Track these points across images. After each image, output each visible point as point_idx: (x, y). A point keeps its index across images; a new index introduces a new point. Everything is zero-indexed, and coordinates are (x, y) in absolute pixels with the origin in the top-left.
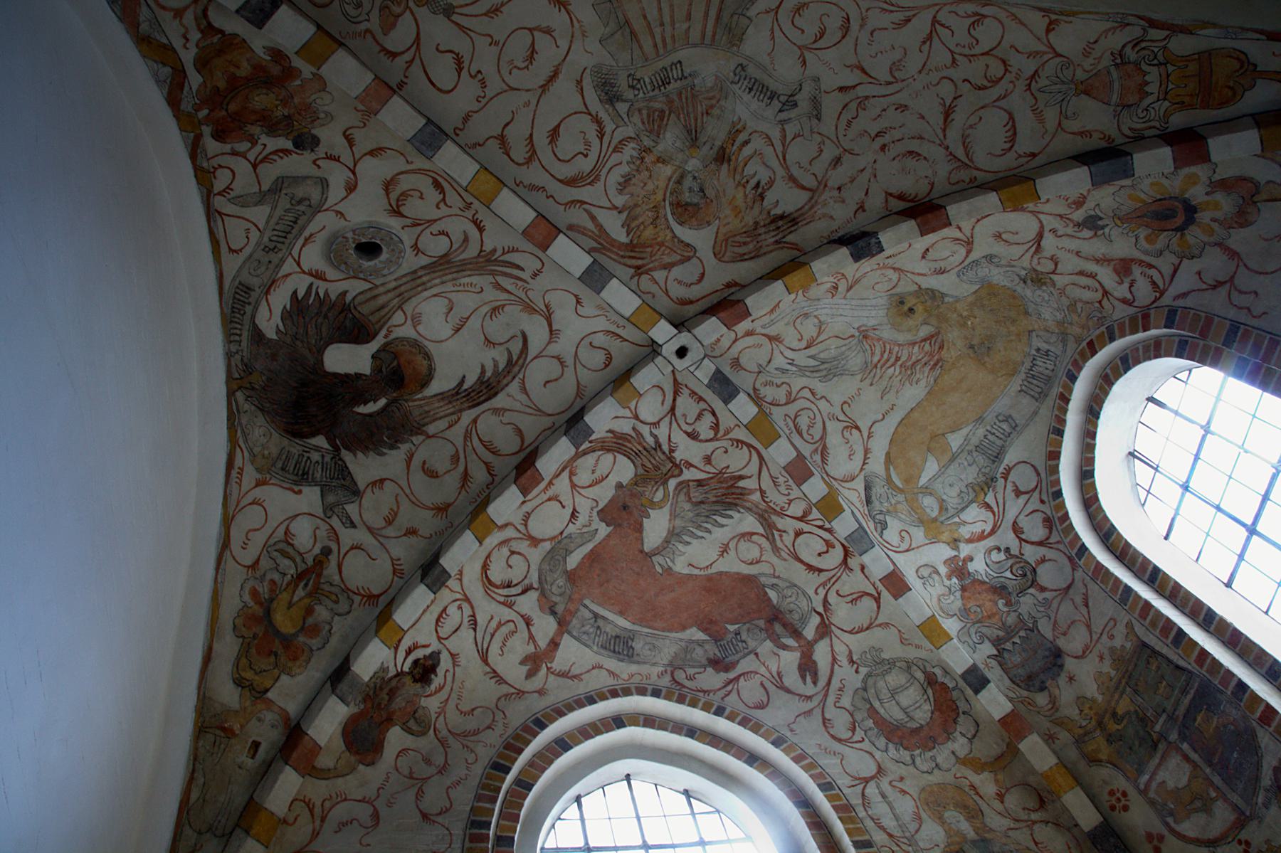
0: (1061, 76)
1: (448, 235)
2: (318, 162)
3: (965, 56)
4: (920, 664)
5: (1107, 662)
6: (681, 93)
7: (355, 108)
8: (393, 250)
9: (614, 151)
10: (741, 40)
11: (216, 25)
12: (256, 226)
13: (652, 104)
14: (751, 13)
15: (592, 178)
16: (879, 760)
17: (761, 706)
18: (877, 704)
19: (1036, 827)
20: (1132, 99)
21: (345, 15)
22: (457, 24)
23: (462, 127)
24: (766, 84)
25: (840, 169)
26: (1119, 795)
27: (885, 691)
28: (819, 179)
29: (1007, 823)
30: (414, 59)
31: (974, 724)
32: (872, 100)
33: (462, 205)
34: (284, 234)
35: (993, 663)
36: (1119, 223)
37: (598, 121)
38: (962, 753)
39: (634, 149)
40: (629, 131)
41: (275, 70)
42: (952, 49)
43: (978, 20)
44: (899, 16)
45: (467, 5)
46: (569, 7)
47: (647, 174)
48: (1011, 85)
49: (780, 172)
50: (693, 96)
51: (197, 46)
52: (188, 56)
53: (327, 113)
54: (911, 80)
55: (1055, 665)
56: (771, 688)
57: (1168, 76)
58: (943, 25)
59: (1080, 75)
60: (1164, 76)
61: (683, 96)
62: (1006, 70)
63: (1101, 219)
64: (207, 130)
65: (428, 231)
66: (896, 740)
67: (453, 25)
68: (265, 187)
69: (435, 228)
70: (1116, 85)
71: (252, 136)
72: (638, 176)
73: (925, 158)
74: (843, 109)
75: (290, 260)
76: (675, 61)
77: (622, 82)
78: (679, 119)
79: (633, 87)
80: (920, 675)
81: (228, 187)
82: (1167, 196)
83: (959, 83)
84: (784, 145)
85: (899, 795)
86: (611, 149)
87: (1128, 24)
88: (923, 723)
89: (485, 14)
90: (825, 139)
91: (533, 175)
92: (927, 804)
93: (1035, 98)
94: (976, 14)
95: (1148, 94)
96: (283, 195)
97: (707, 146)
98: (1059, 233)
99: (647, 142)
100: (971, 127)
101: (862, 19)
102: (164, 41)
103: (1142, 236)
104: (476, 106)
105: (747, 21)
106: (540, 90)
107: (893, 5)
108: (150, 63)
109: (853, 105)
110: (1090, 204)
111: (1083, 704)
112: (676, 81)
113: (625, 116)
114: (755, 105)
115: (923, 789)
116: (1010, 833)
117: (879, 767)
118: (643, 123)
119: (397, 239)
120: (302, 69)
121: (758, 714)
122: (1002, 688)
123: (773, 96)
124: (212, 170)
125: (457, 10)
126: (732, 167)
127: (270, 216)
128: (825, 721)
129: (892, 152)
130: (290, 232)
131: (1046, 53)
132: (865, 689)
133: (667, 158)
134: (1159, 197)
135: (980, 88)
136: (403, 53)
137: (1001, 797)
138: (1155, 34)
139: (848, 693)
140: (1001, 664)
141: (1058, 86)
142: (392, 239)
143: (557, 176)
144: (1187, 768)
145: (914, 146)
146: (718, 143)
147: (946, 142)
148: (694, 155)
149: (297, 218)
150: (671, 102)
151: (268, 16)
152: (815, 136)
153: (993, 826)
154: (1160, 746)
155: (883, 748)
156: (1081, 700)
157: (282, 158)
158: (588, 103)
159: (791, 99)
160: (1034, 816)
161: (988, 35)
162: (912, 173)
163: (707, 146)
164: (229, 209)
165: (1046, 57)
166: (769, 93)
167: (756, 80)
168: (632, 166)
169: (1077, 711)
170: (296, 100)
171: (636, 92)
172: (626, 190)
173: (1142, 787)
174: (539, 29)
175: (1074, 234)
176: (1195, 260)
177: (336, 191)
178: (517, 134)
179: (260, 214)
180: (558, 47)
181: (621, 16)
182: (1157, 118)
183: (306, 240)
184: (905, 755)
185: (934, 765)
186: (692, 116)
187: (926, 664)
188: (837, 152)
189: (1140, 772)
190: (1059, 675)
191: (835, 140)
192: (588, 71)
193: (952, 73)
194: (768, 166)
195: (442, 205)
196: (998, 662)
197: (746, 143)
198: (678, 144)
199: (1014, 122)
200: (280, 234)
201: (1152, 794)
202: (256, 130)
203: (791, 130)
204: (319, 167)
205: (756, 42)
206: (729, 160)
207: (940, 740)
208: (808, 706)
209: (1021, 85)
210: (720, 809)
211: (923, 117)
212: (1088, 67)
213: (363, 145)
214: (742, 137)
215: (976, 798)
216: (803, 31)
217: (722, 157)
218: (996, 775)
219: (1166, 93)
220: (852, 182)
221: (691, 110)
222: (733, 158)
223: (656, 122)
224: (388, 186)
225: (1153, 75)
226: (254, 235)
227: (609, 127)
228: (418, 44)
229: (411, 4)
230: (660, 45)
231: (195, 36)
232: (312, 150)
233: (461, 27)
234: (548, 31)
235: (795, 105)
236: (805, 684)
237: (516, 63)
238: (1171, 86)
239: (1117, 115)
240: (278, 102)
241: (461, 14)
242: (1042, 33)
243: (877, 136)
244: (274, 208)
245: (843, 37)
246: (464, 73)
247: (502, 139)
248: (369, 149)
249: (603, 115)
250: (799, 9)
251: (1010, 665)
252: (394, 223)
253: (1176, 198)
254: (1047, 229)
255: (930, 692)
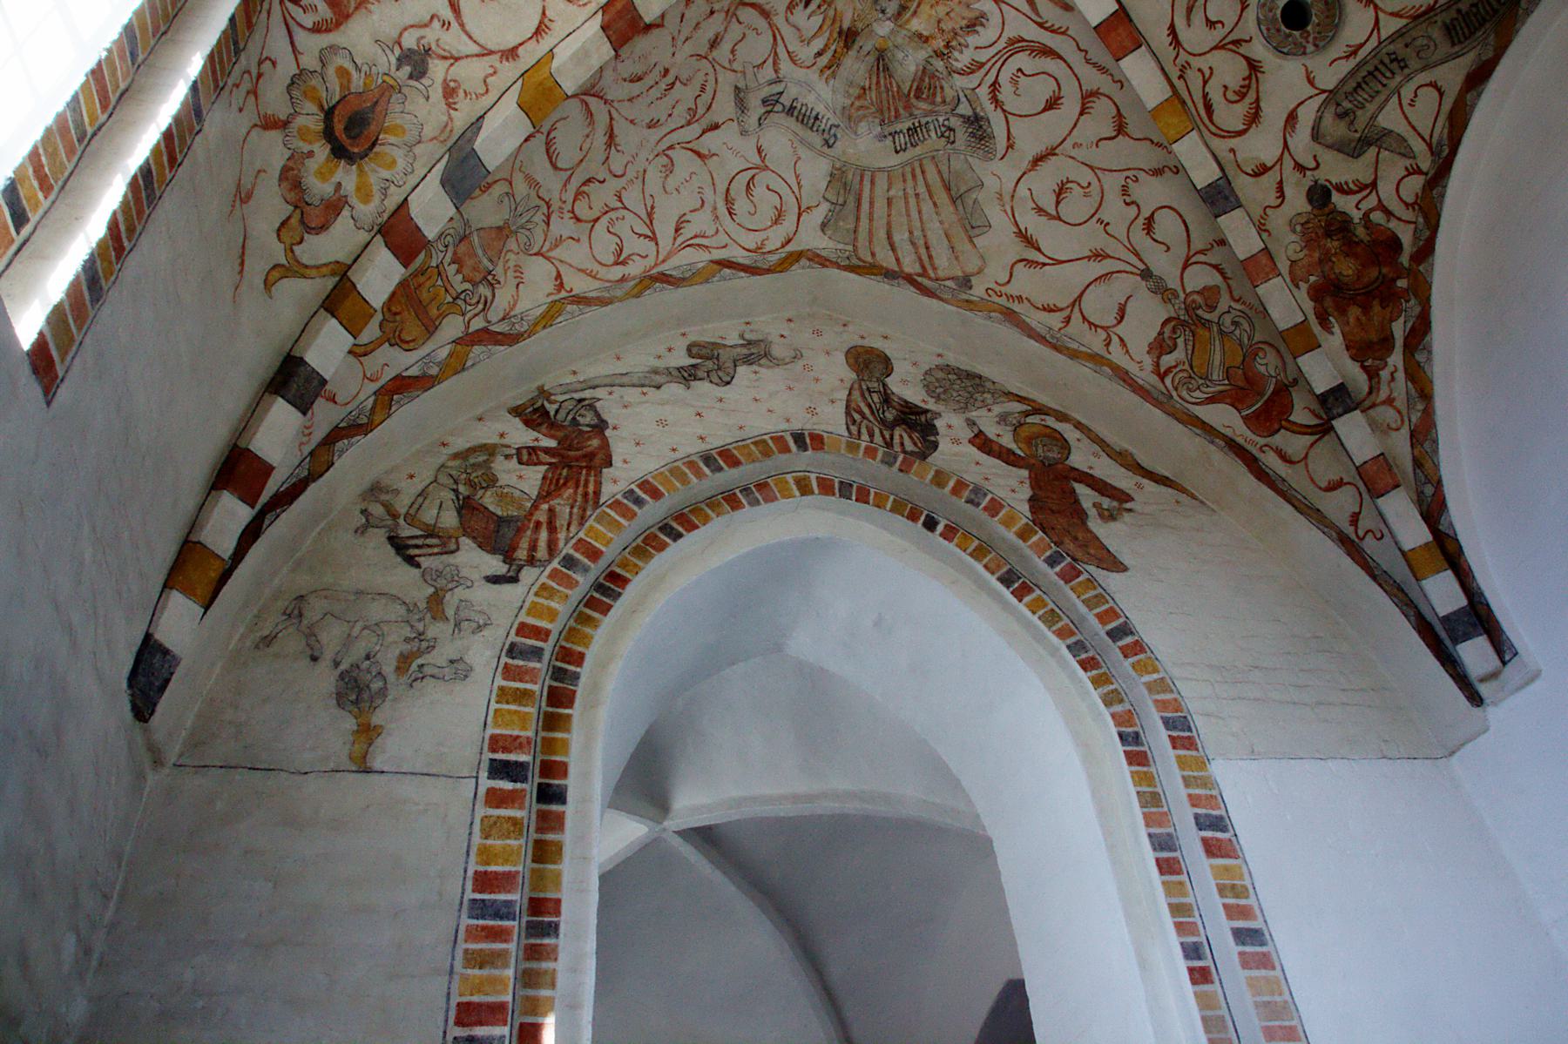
0: (528, 233)
1: (1207, 19)
2: (1313, 165)
3: (613, 210)
6: (896, 117)
7: (1270, 235)
8: (1270, 11)
9: (982, 65)
10: (831, 175)
11: (1365, 377)
12: (1400, 104)
13: (930, 107)
14: (825, 207)
15: (1017, 45)
20: (462, 248)
21: (1252, 325)
22: (1141, 260)
23: (1166, 169)
24: (799, 124)
25: (711, 35)
28: (734, 20)
30: (1196, 254)
32: (683, 122)
33: (1189, 73)
34: (1376, 73)
36: (392, 82)
37: (997, 102)
39: (957, 60)
40: (960, 82)
41: (1328, 302)
42: (626, 211)
43: (619, 256)
44: (688, 232)
45: (1127, 272)
46: (1016, 230)
47: (942, 25)
48: (564, 199)
49: (779, 21)
50: (881, 111)
51: (1386, 364)
52: (1396, 359)
53: (1294, 231)
54: (651, 158)
57: (446, 290)
58: (646, 237)
59: (512, 244)
60: (449, 287)
61: (893, 113)
62: (573, 212)
63: (411, 77)
64: (1405, 260)
65: (1227, 29)
67: (1146, 261)
68: (1373, 150)
69: (1219, 32)
70: (480, 252)
71: (1367, 228)
72: (957, 27)
73: (625, 80)
74: (711, 104)
75: (1384, 35)
76: (901, 153)
77: (962, 136)
78: (899, 87)
79: (951, 129)
81: (1410, 174)
82: (371, 155)
83: (609, 177)
84: (776, 53)
86: (987, 67)
87: (503, 319)
89: (1109, 256)
90: (727, 65)
91: (1092, 79)
93: (539, 197)
94: (624, 263)
95: (453, 262)
96: (1360, 130)
97: (864, 52)
98: (436, 24)
99: (939, 64)
100: (588, 136)
101: (717, 217)
102: (1409, 383)
103: (353, 72)
104: (1141, 175)
105: (828, 196)
106: (1057, 151)
107: (698, 245)
108: (1429, 374)
109: (700, 111)
110: (437, 93)
112: (901, 131)
113: (963, 99)
114: (810, 100)
118: (942, 88)
119: (1263, 28)
120: (1306, 295)
123: (790, 111)
124: (1416, 207)
125: (1139, 272)
126: (837, 25)
127: (1381, 108)
129: (659, 68)
130: (1370, 73)
131: (548, 251)
133: (916, 39)
134: (377, 149)
135: (589, 181)
136: (1205, 263)
138: (477, 324)
141: (524, 221)
142: (1268, 30)
143: (1064, 65)
145: (636, 88)
146: (852, 53)
147: (608, 106)
148: (881, 40)
149: (1355, 90)
150: (908, 107)
151: (1332, 391)
152: (740, 69)
157: (1346, 183)
158: (1004, 122)
159: (769, 108)
161: (604, 245)
162: (637, 59)
163: (864, 52)
164: (1418, 146)
165: (547, 245)
166: (796, 113)
167: (811, 128)
168: (963, 41)
170: (1316, 255)
171: (946, 123)
172: (972, 15)
174: (1051, 217)
175: (422, 32)
176: (289, 81)
177: (1307, 116)
178: (1099, 122)
179: (1390, 118)
180: (1030, 189)
181: (960, 208)
182: (434, 245)
183: (1355, 53)
186: (883, 88)
188: (715, 53)
191: (717, 67)
192: (999, 155)
193: (616, 184)
194: (794, 26)
195: (1207, 75)
197: (819, 54)
198: (900, 55)
199: (551, 162)
200: (1379, 76)
202: (1361, 232)
203: (768, 73)
204: (1315, 157)
205: (816, 172)
206: (840, 33)
209: (556, 204)
211: (632, 122)
212: (511, 256)
213: (1270, 180)
214: (824, 60)
216: (768, 188)
217: (849, 37)
219: (439, 274)
220: (698, 24)
221: (884, 95)
222: (835, 35)
223: (926, 86)
224: (1254, 117)
225: (458, 283)
226: (1407, 92)
227: (984, 92)
228: (1187, 261)
229: (1182, 296)
230: (918, 171)
231: (1384, 374)
232: (1316, 182)
233: (1137, 255)
234: (1040, 210)
235: (764, 102)
237: (1082, 190)
238: (440, 282)
239: (467, 224)
240: (1334, 259)
241: (1135, 267)
242: (563, 269)
243: (673, 84)
244: (1374, 117)
245: (728, 190)
246: (1146, 213)
247: (1121, 129)
248: (1266, 175)
249: (990, 107)
250: (779, 216)
252: (1259, 50)
253: (362, 158)
254: (455, 24)
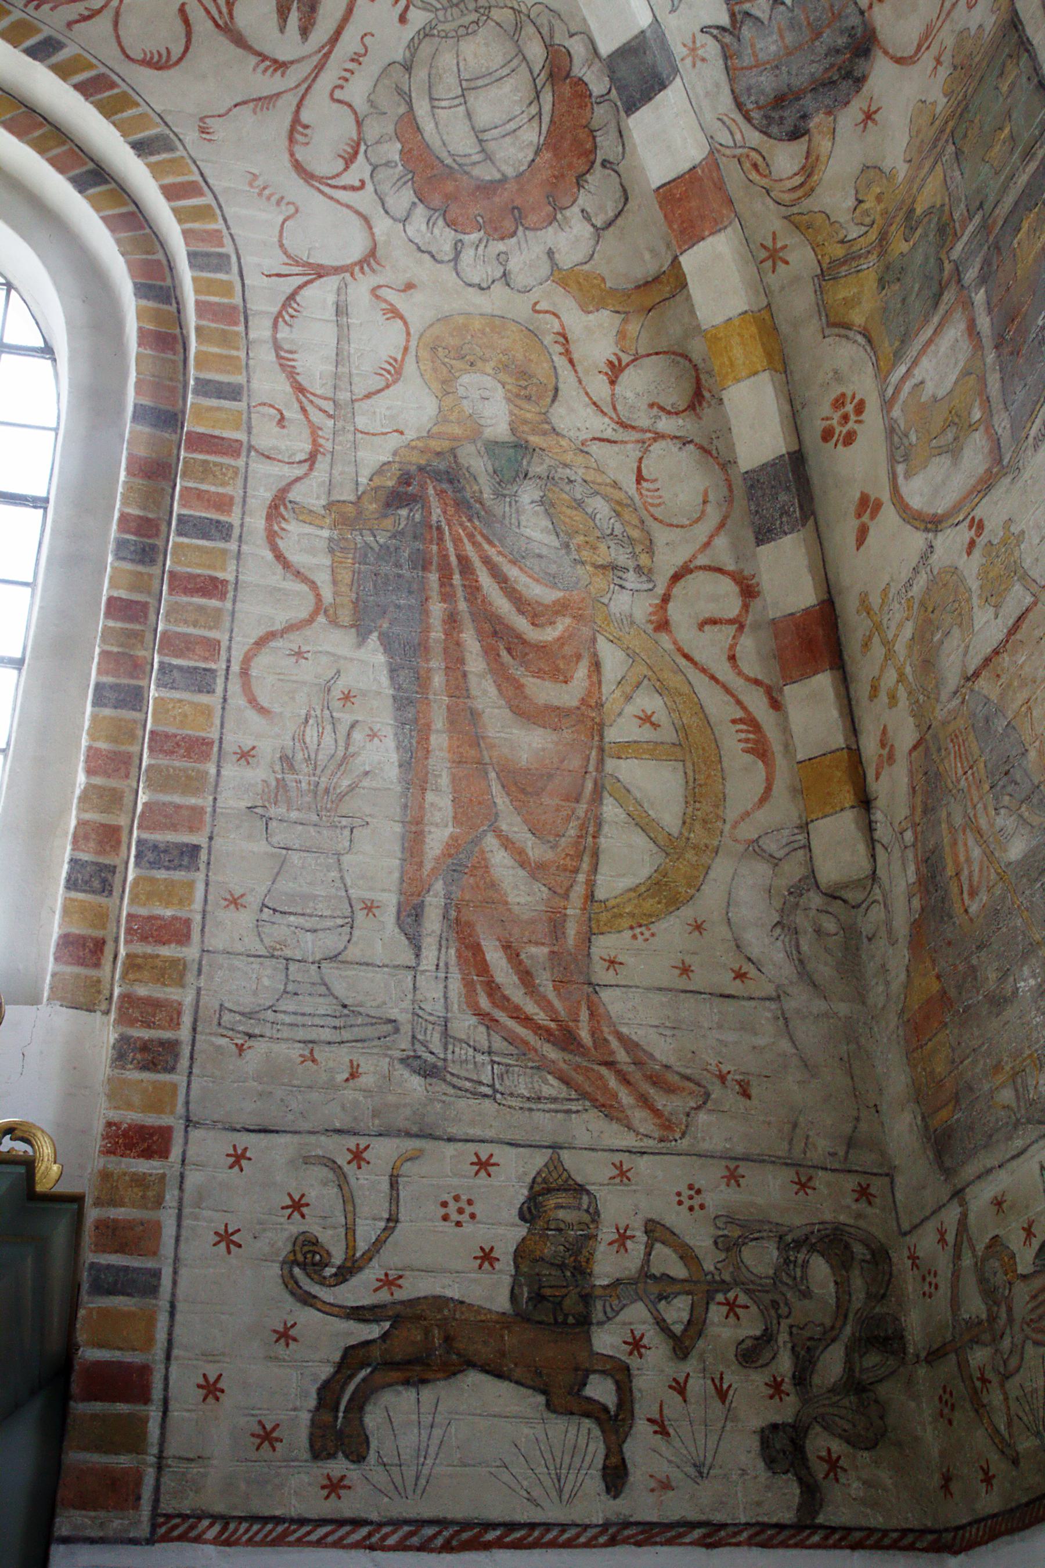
4: (543, 20)
5: (943, 72)
16: (380, 238)
17: (159, 63)
18: (422, 109)
19: (657, 447)
26: (849, 408)
27: (451, 80)
29: (603, 426)
31: (619, 193)
35: (711, 48)
38: (567, 259)
55: (848, 75)
56: (202, 25)
66: (437, 201)
80: (536, 52)
85: (380, 318)
88: (510, 172)
92: (434, 349)
111: (868, 186)
115: (445, 319)
116: (594, 448)
117: (373, 253)
121: (144, 79)
122: (709, 117)
128: (297, 126)
132: (408, 67)
137: (615, 371)
139: (372, 67)
140: (727, 56)
144: (965, 347)
153: (561, 426)
154: (946, 297)
155: (401, 213)
156: (871, 171)
160: (666, 424)
169: (851, 202)
173: (890, 391)
184: (444, 238)
185: (498, 274)
187: (557, 23)
189: (898, 356)
190: (847, 103)
196: (724, 47)
201: (896, 413)
207: (532, 219)
208: (274, 83)
210: (15, 282)
215: (561, 362)
218: (625, 321)
236: (282, 30)
251: (747, 61)
255: (547, 98)
